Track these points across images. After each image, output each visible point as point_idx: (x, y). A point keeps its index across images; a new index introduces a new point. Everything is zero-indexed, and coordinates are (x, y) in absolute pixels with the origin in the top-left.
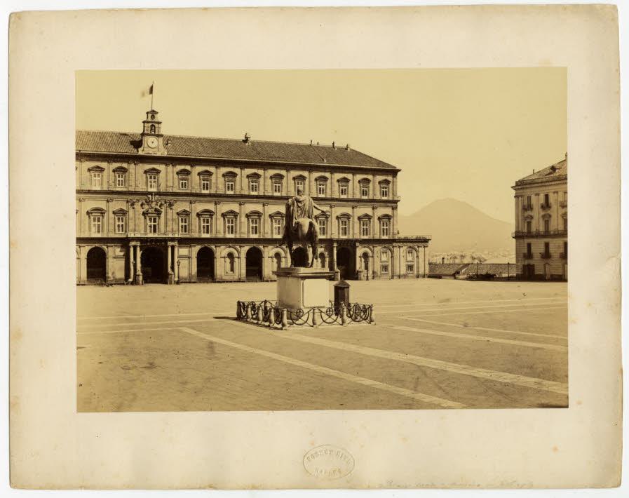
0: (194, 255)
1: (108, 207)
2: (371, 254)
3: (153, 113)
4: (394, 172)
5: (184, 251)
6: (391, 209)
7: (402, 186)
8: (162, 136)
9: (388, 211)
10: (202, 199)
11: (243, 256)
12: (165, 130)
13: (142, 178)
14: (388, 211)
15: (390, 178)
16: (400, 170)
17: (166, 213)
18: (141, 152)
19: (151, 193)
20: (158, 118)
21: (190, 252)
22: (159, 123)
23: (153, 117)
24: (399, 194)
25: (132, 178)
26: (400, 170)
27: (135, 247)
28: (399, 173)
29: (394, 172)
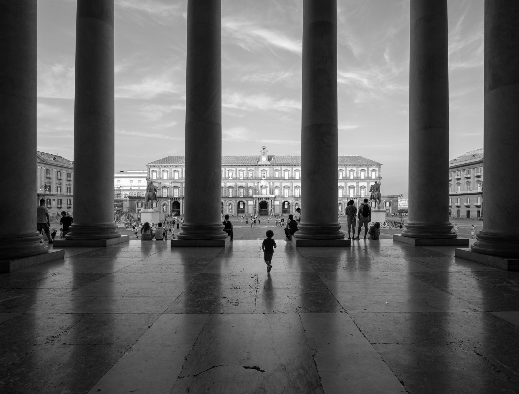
5: (277, 203)
15: (377, 169)
18: (259, 163)
20: (266, 150)
23: (264, 149)
29: (379, 165)
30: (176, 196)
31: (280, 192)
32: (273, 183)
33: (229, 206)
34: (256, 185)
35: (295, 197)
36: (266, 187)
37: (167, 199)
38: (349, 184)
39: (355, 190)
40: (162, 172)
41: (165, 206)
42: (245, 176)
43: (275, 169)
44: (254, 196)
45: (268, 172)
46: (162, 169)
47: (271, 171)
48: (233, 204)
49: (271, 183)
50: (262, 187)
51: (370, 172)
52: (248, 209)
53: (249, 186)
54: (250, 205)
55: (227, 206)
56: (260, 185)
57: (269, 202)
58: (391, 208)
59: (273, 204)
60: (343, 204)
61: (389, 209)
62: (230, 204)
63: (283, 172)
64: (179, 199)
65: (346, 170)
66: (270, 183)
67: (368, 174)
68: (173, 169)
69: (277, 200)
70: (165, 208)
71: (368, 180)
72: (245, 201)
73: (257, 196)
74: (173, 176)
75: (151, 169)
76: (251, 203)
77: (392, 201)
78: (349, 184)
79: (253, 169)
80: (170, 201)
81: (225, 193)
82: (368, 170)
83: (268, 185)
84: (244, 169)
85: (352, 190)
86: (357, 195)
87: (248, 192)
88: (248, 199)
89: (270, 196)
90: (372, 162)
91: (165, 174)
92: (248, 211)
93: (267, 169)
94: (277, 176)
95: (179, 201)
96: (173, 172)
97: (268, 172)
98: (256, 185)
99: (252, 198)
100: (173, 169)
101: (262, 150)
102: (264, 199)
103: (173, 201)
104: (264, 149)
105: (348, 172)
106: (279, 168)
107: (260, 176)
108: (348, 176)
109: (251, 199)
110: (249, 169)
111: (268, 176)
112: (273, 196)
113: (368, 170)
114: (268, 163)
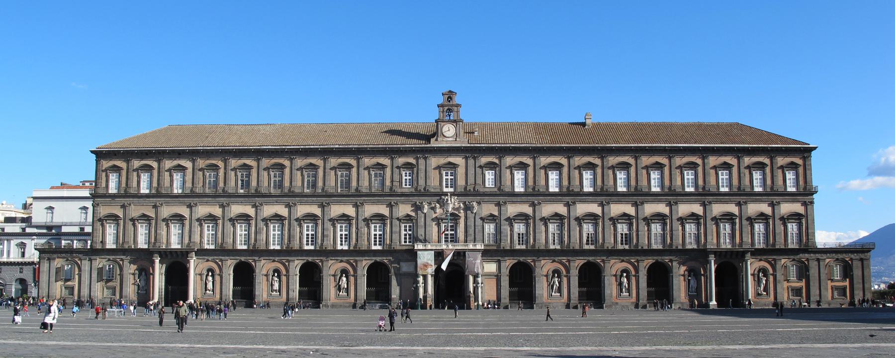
0: (505, 272)
1: (391, 212)
3: (450, 95)
4: (805, 152)
5: (491, 267)
6: (799, 204)
8: (461, 121)
9: (798, 208)
10: (514, 199)
11: (574, 273)
12: (466, 115)
13: (434, 175)
15: (799, 161)
16: (815, 148)
17: (466, 218)
18: (434, 144)
19: (446, 194)
20: (457, 100)
22: (458, 106)
23: (450, 99)
24: (815, 183)
25: (422, 175)
26: (815, 148)
29: (805, 152)
32: (479, 203)
45: (461, 171)
75: (106, 164)
89: (471, 247)
93: (458, 160)
97: (461, 171)
101: (441, 100)
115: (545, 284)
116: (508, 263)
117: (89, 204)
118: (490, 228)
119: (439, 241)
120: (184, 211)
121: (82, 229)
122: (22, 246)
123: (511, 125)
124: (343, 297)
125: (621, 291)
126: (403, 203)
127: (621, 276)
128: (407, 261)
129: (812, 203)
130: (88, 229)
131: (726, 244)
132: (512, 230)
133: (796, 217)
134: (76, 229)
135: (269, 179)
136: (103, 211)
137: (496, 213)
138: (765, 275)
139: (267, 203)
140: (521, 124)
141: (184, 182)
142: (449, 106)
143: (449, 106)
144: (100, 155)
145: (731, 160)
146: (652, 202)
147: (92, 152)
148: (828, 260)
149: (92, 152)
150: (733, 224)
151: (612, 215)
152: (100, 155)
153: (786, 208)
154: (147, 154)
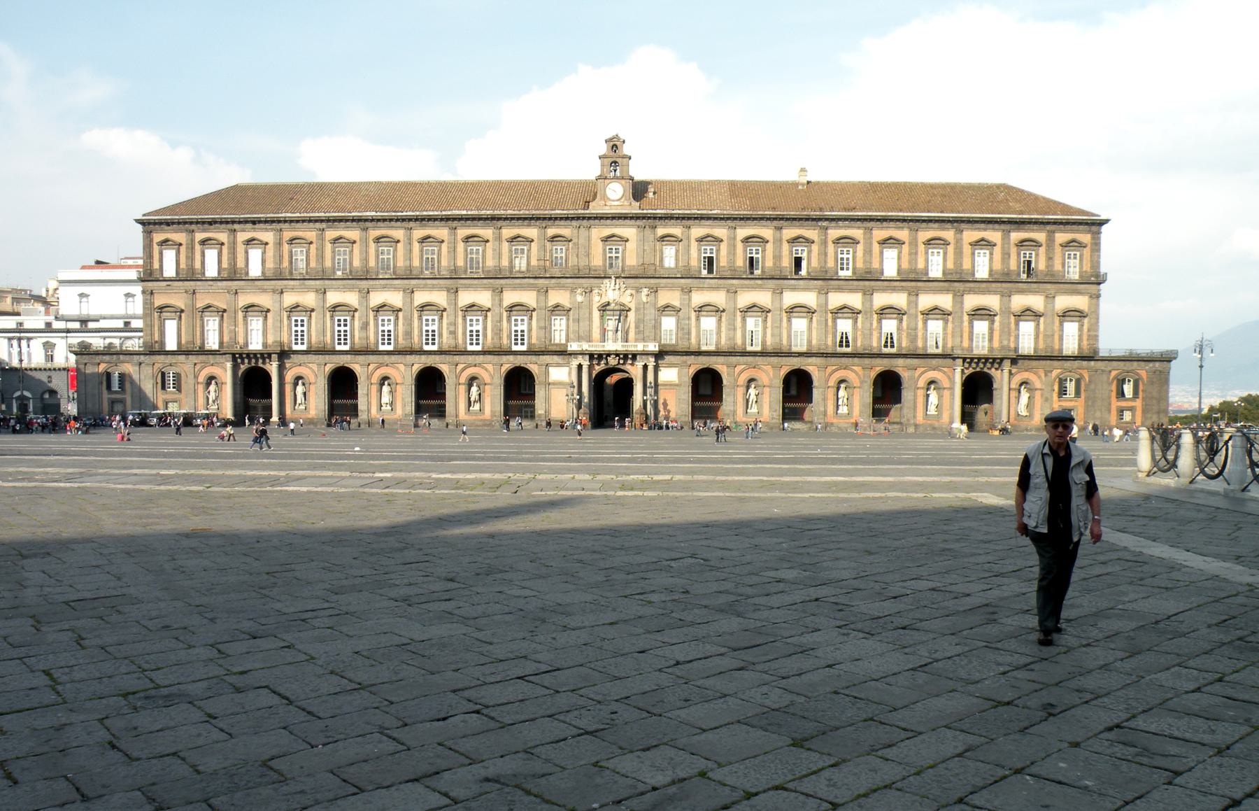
2: (1038, 385)
3: (614, 145)
4: (1095, 225)
5: (669, 375)
7: (1114, 248)
9: (1080, 302)
14: (1080, 302)
15: (1085, 238)
16: (1106, 221)
18: (595, 208)
20: (626, 150)
21: (679, 377)
23: (614, 148)
26: (1106, 221)
27: (580, 367)
28: (1104, 228)
29: (1095, 225)
30: (256, 345)
31: (683, 330)
33: (470, 386)
34: (580, 298)
35: (745, 354)
36: (623, 311)
37: (219, 359)
38: (971, 301)
39: (997, 324)
40: (198, 247)
41: (212, 388)
42: (534, 262)
43: (661, 231)
44: (573, 347)
45: (631, 246)
46: (200, 236)
47: (643, 240)
48: (488, 380)
49: (645, 291)
50: (604, 308)
51: (1058, 249)
52: (547, 400)
53: (551, 302)
54: (559, 384)
55: (462, 389)
56: (597, 300)
57: (635, 370)
58: (1138, 404)
59: (650, 378)
60: (946, 383)
61: (1131, 409)
62: (472, 379)
63: (694, 245)
64: (265, 356)
65: (959, 242)
66: (638, 290)
67: (1050, 259)
68: (242, 236)
69: (671, 365)
70: (212, 396)
71: (1049, 286)
72: (534, 369)
73: (586, 346)
74: (240, 263)
75: (158, 237)
76: (561, 373)
77: (1143, 374)
78: (971, 301)
79: (566, 231)
80: (229, 365)
81: (453, 333)
82: (1051, 240)
83: (626, 299)
84: (531, 232)
85: (981, 327)
86: (1002, 348)
87: (547, 329)
88: (547, 359)
89: (640, 347)
90: (1066, 209)
91: (211, 255)
92: (547, 412)
93: (628, 230)
94: (669, 257)
95: (267, 367)
96: (240, 248)
98: (580, 298)
99: (563, 352)
100: (242, 236)
101: (603, 149)
102: (613, 361)
103: (243, 368)
104: (614, 148)
105: (967, 249)
106: (677, 231)
107: (597, 261)
108: (966, 265)
109: (556, 359)
110: (551, 232)
111: (632, 261)
112: (653, 347)
113: (1051, 240)
114: (635, 208)
115: (740, 400)
116: (692, 371)
117: (137, 289)
118: (668, 323)
119: (603, 339)
120: (264, 300)
121: (127, 324)
122: (49, 346)
123: (701, 183)
124: (475, 413)
125: (838, 406)
126: (553, 288)
127: (838, 389)
128: (559, 365)
129: (1098, 296)
130: (137, 324)
131: (981, 347)
132: (698, 326)
133: (1078, 314)
134: (119, 324)
135: (377, 256)
136: (159, 301)
137: (677, 303)
138: (1029, 390)
139: (375, 289)
140: (712, 183)
141: (263, 261)
142: (615, 155)
143: (615, 155)
144: (149, 225)
145: (994, 235)
146: (884, 290)
147: (138, 221)
148: (1114, 373)
149: (138, 221)
150: (992, 322)
151: (830, 307)
152: (149, 225)
153: (1064, 302)
154: (210, 223)
